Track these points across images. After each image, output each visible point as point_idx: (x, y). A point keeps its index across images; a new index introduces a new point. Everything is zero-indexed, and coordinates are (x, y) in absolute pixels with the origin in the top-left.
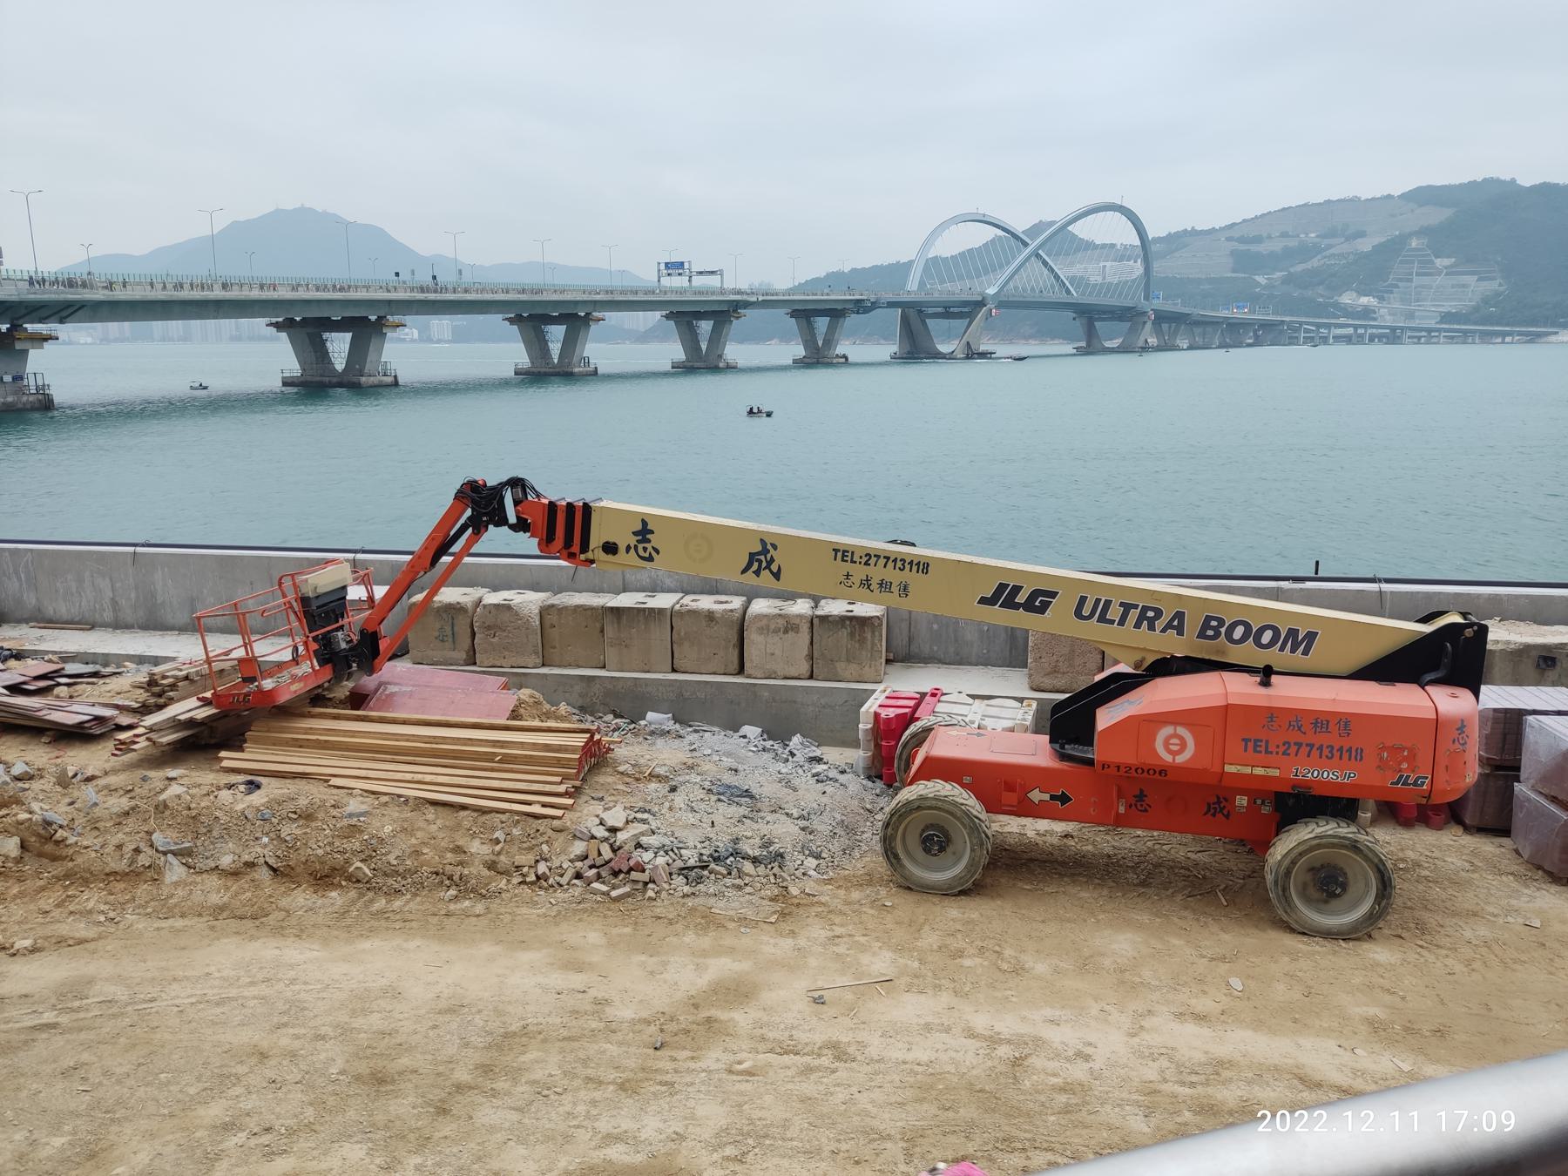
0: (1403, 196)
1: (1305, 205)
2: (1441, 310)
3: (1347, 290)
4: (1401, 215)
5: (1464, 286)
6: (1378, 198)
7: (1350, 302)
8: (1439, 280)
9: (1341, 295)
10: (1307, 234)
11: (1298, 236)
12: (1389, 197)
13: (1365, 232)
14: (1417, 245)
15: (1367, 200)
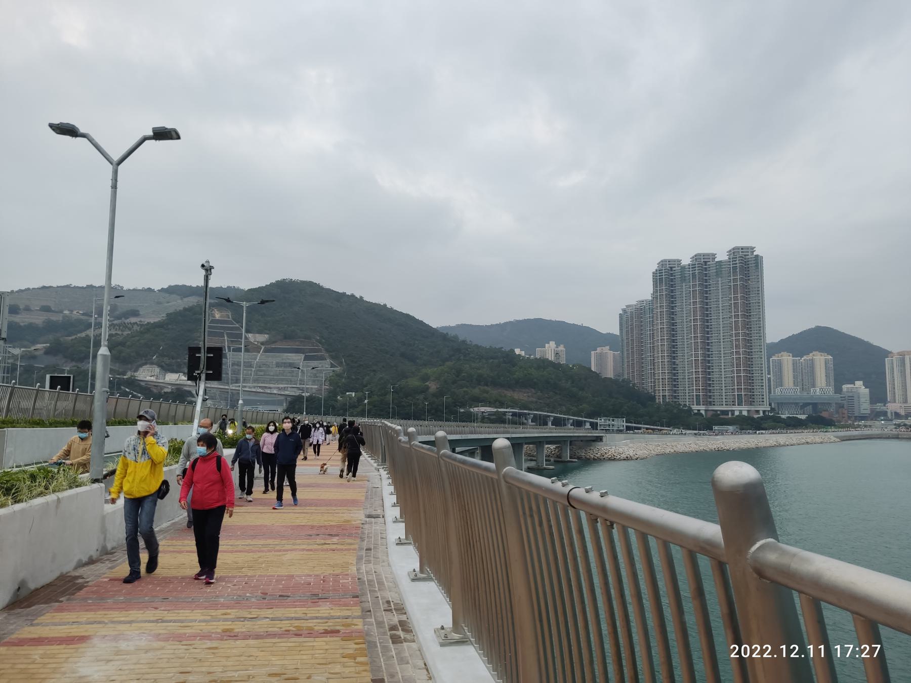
0: (162, 290)
1: (68, 287)
2: (287, 393)
3: (145, 364)
4: (168, 302)
5: (291, 365)
6: (140, 290)
7: (153, 379)
8: (259, 357)
9: (136, 370)
10: (71, 311)
11: (61, 312)
12: (149, 289)
13: (138, 311)
14: (221, 317)
15: (129, 290)
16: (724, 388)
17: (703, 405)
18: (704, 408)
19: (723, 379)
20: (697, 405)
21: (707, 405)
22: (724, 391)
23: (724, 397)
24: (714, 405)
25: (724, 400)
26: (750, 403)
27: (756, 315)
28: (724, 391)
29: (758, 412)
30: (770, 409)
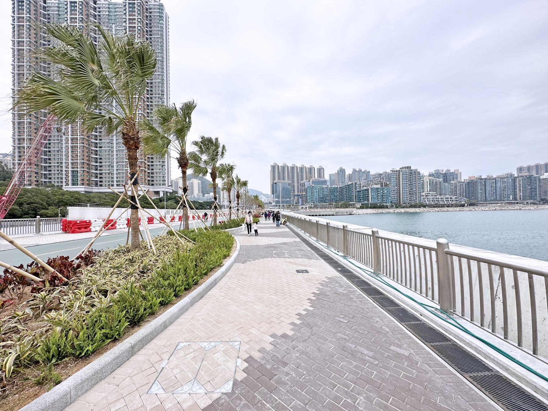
16: (115, 164)
17: (83, 184)
18: (83, 189)
19: (115, 153)
20: (73, 184)
21: (88, 185)
22: (115, 168)
23: (115, 176)
24: (101, 185)
25: (115, 179)
26: (147, 181)
27: (159, 75)
28: (115, 168)
29: (157, 193)
30: (171, 191)
